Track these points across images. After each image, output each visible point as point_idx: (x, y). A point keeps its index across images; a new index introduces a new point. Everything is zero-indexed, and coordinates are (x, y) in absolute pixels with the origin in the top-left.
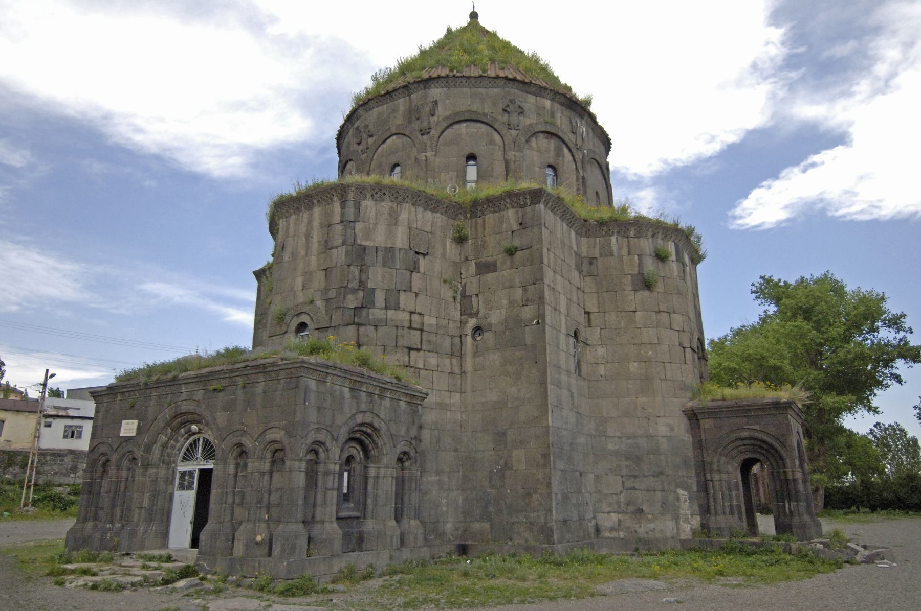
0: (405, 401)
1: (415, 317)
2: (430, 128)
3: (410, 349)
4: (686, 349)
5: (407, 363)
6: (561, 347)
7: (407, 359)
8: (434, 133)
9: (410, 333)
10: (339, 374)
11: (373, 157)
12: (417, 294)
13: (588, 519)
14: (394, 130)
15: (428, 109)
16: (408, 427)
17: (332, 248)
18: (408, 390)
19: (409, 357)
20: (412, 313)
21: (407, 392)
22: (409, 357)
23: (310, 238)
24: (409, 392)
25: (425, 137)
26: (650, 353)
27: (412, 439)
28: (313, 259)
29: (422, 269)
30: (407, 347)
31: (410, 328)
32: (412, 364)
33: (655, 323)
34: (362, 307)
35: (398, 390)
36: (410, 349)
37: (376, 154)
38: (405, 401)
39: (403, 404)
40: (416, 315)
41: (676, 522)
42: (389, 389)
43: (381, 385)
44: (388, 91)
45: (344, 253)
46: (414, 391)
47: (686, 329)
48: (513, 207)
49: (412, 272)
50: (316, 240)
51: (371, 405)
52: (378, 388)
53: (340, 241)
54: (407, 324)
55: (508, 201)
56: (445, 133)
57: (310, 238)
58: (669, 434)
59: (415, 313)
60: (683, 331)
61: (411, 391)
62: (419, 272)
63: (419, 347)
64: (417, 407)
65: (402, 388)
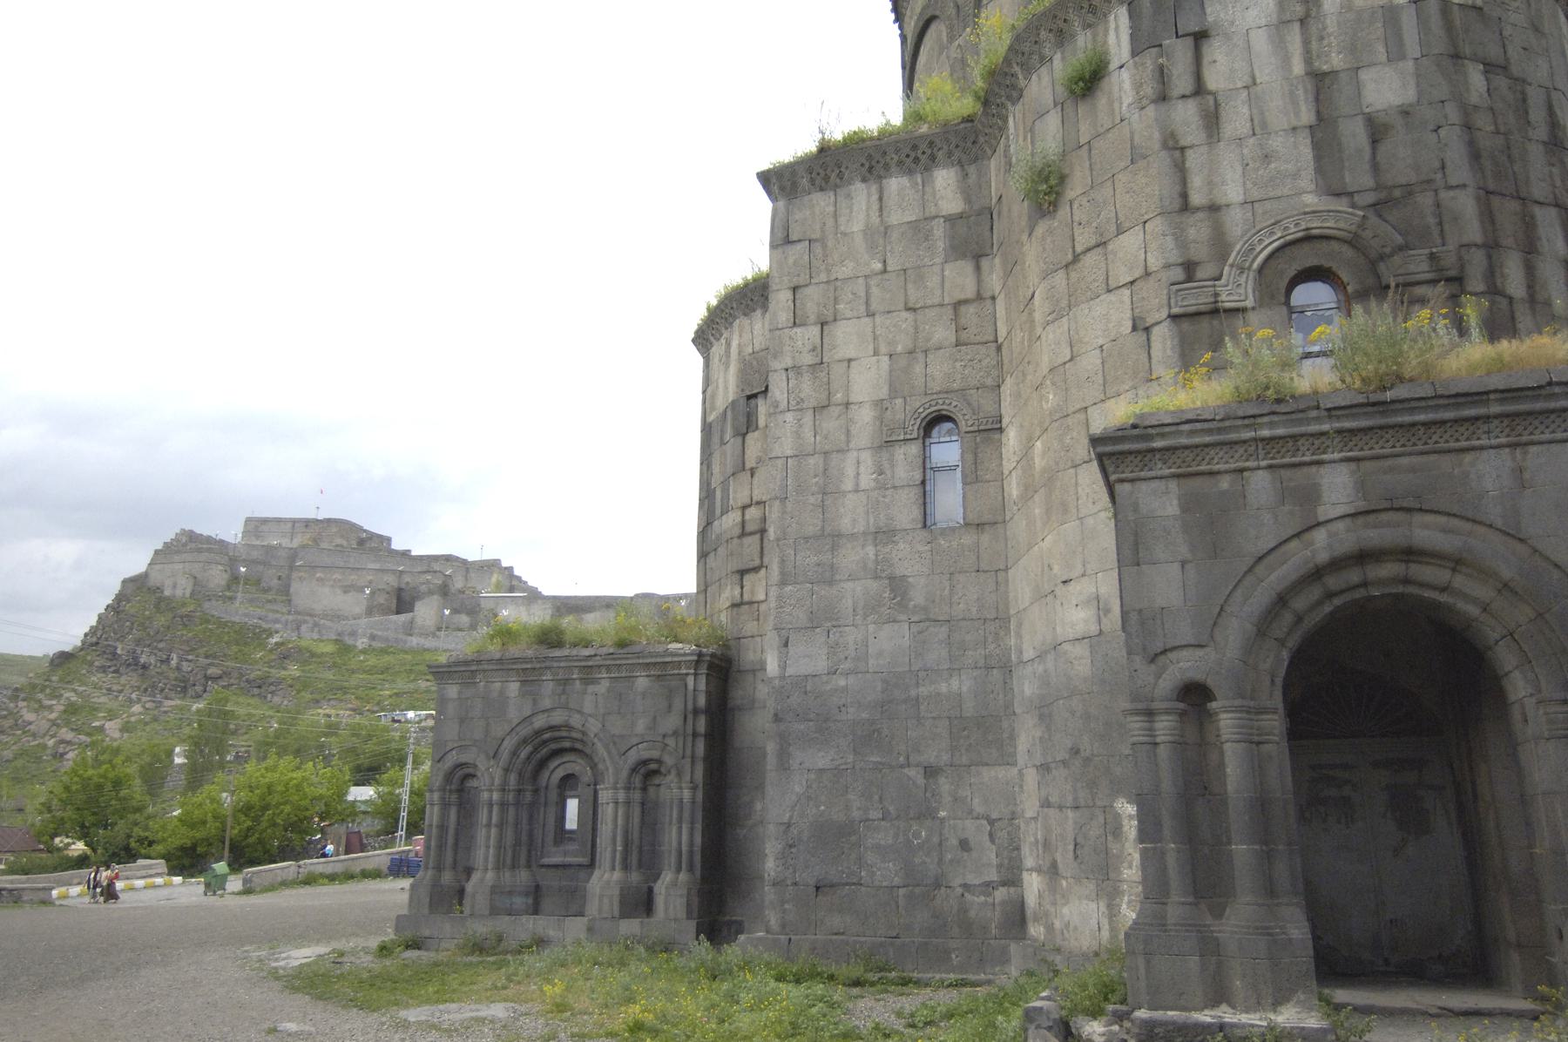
0: (647, 676)
1: (752, 513)
3: (742, 573)
4: (1156, 331)
5: (738, 599)
6: (848, 485)
7: (737, 591)
9: (741, 545)
10: (491, 667)
12: (753, 472)
13: (965, 886)
16: (655, 718)
18: (643, 657)
19: (742, 588)
20: (744, 508)
21: (641, 661)
22: (742, 588)
24: (648, 661)
26: (1051, 397)
27: (664, 736)
29: (762, 422)
30: (738, 572)
31: (743, 534)
32: (746, 598)
33: (1064, 303)
34: (708, 524)
35: (618, 662)
36: (742, 573)
38: (647, 676)
39: (642, 682)
40: (753, 508)
41: (1110, 906)
42: (599, 666)
43: (576, 664)
46: (663, 656)
47: (1154, 262)
49: (744, 435)
51: (563, 697)
52: (576, 671)
54: (737, 531)
58: (1094, 629)
59: (750, 506)
60: (1147, 274)
61: (652, 657)
62: (757, 428)
63: (757, 562)
64: (685, 680)
65: (627, 658)
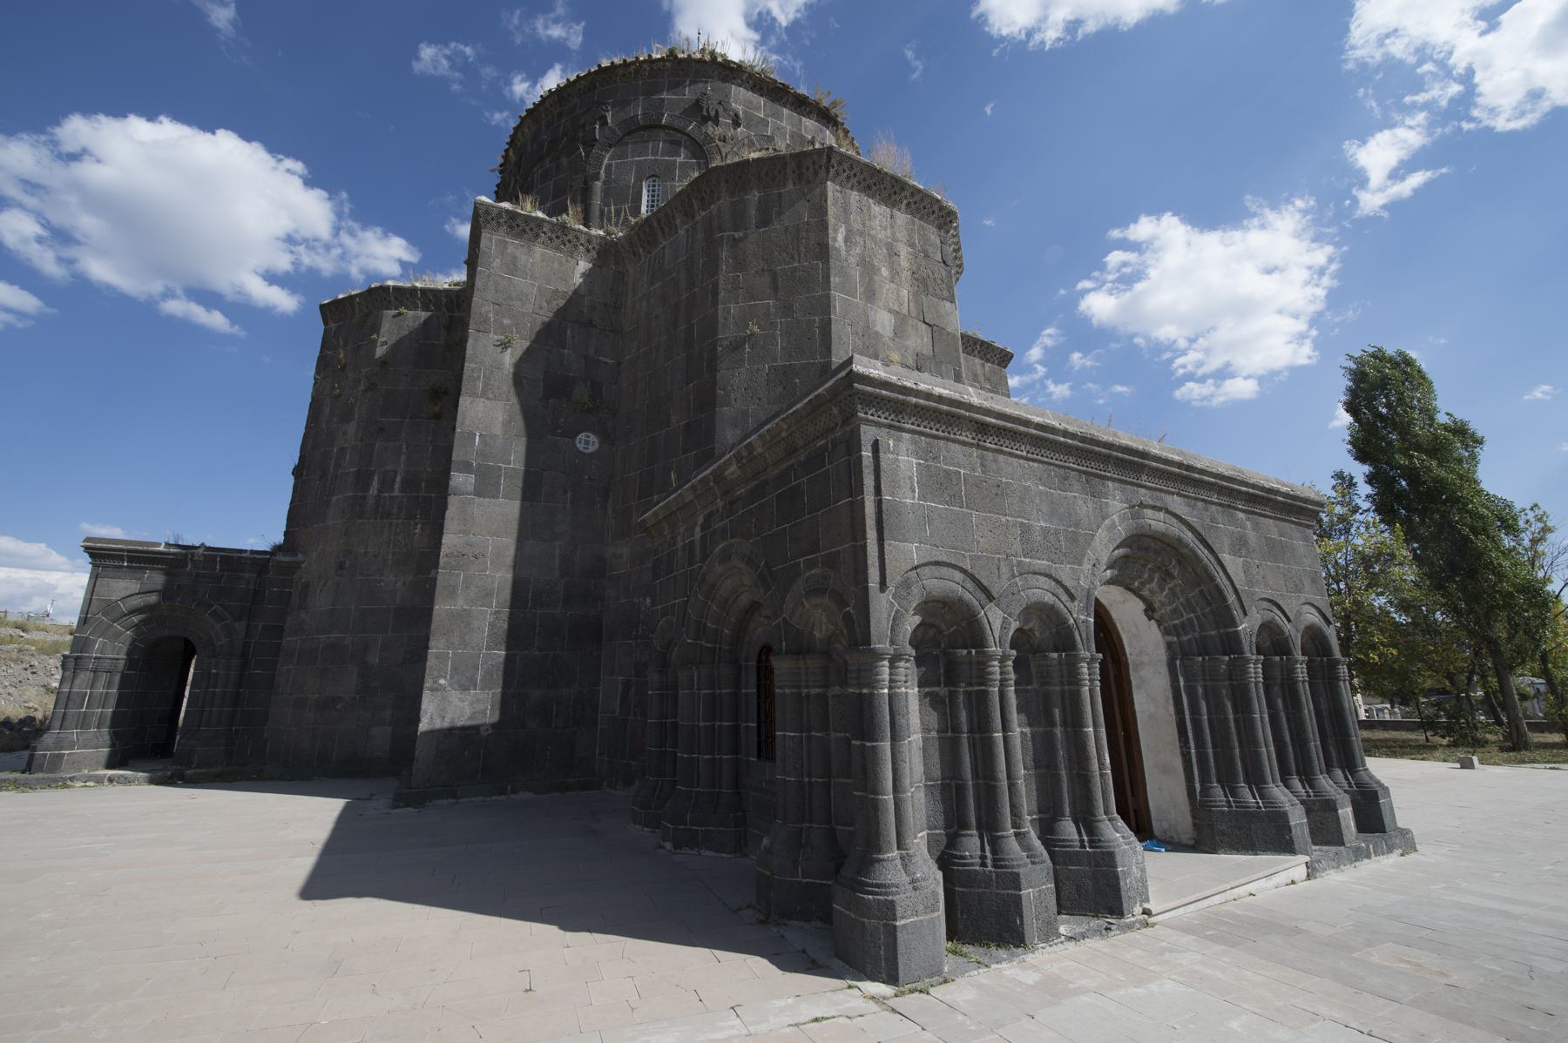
48: (980, 358)
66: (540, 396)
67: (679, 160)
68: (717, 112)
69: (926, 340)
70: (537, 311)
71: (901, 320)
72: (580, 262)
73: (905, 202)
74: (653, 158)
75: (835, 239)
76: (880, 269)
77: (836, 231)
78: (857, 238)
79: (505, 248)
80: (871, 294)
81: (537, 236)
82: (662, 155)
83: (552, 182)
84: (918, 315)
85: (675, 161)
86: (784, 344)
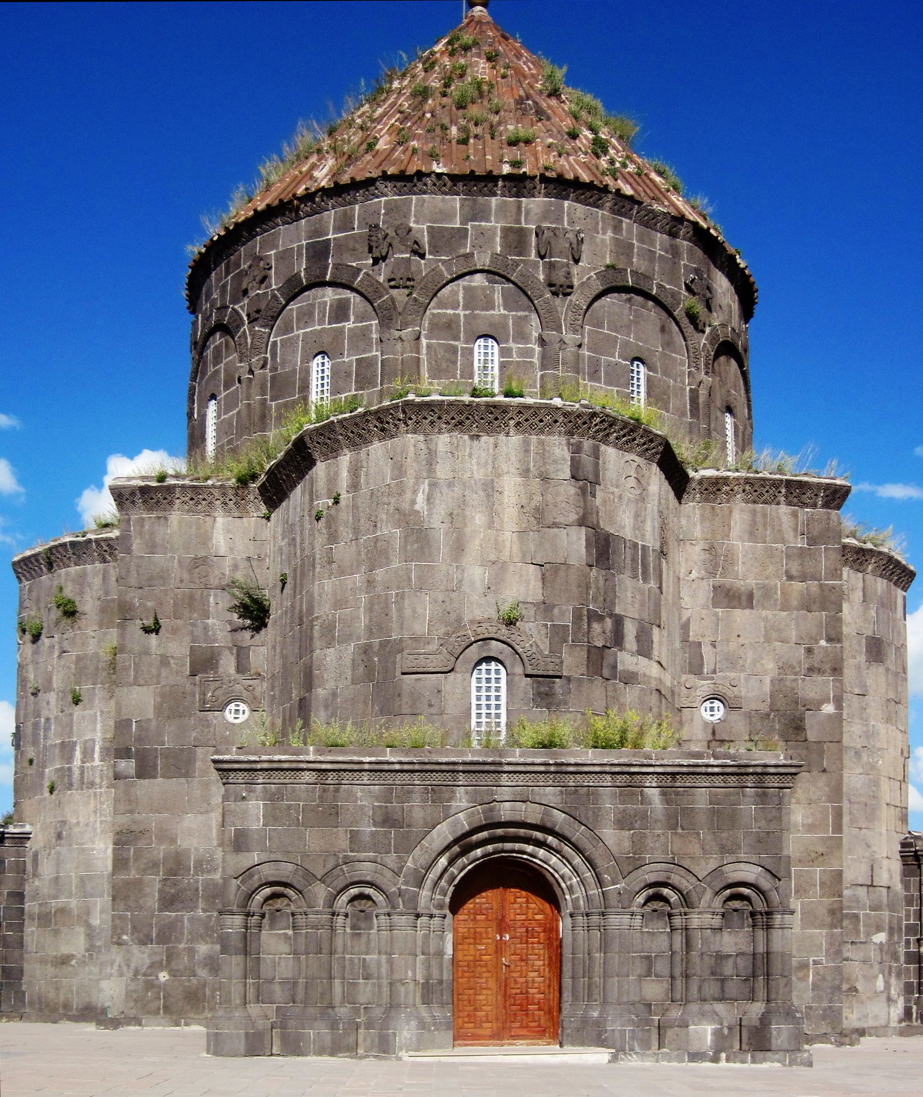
2: (571, 287)
8: (578, 298)
11: (429, 304)
14: (483, 260)
15: (567, 245)
17: (555, 525)
23: (496, 495)
25: (558, 301)
28: (509, 537)
37: (435, 299)
44: (472, 172)
45: (584, 543)
50: (514, 500)
53: (573, 517)
55: (783, 490)
56: (596, 304)
57: (496, 495)
66: (188, 673)
67: (349, 325)
68: (390, 245)
69: (533, 583)
70: (179, 585)
71: (498, 568)
72: (218, 519)
73: (512, 422)
74: (319, 328)
75: (413, 502)
76: (473, 518)
77: (415, 492)
78: (445, 490)
79: (142, 526)
80: (459, 549)
81: (171, 503)
82: (330, 323)
83: (222, 365)
84: (524, 556)
85: (342, 330)
86: (367, 622)
